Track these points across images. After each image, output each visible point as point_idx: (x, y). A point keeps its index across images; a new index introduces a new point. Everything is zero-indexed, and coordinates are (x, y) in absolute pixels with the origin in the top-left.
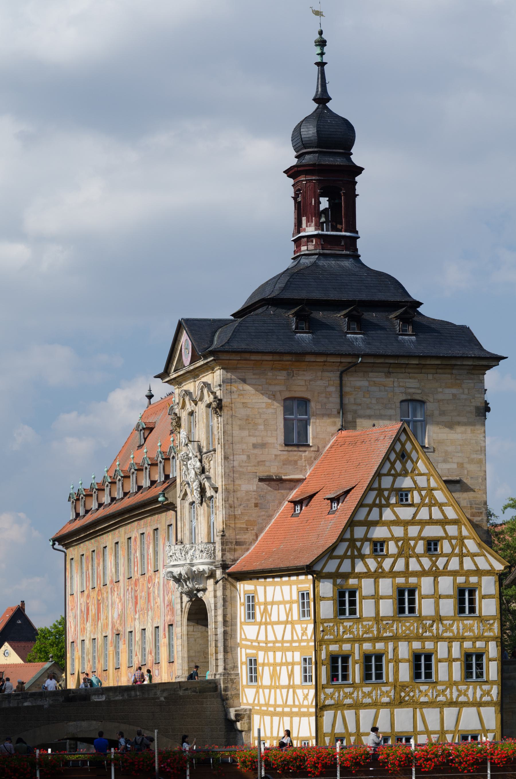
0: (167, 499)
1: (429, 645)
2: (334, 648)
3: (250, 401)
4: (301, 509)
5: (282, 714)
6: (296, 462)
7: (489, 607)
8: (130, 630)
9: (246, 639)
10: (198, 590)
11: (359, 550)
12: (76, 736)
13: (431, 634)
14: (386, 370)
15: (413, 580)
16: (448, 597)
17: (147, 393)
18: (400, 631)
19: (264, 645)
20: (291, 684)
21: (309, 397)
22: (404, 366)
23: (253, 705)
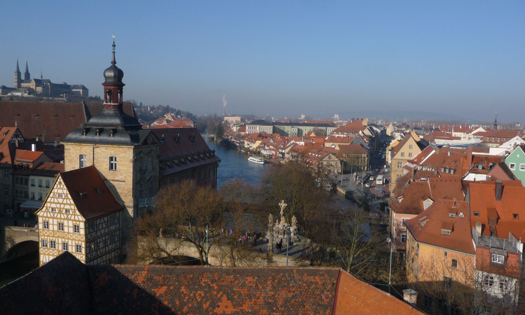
1: (67, 240)
2: (43, 237)
7: (82, 232)
15: (62, 221)
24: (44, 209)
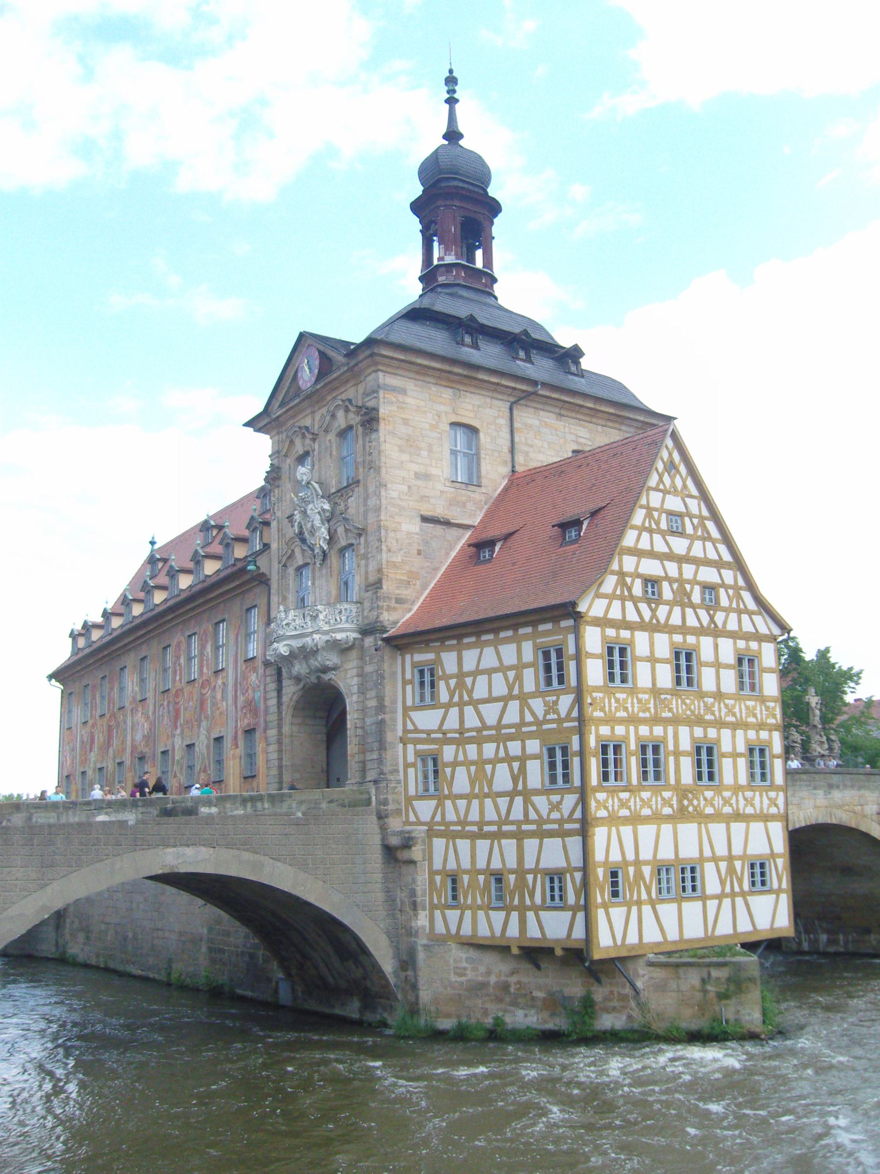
0: (258, 568)
1: (712, 733)
2: (605, 730)
3: (411, 417)
4: (493, 552)
5: (499, 835)
6: (464, 505)
7: (771, 685)
8: (163, 750)
9: (416, 730)
10: (325, 670)
11: (629, 589)
12: (176, 870)
13: (712, 717)
14: (557, 410)
15: (691, 639)
16: (728, 666)
17: (150, 539)
18: (680, 711)
19: (457, 735)
20: (520, 787)
21: (478, 426)
22: (577, 408)
23: (430, 824)
24: (610, 583)
